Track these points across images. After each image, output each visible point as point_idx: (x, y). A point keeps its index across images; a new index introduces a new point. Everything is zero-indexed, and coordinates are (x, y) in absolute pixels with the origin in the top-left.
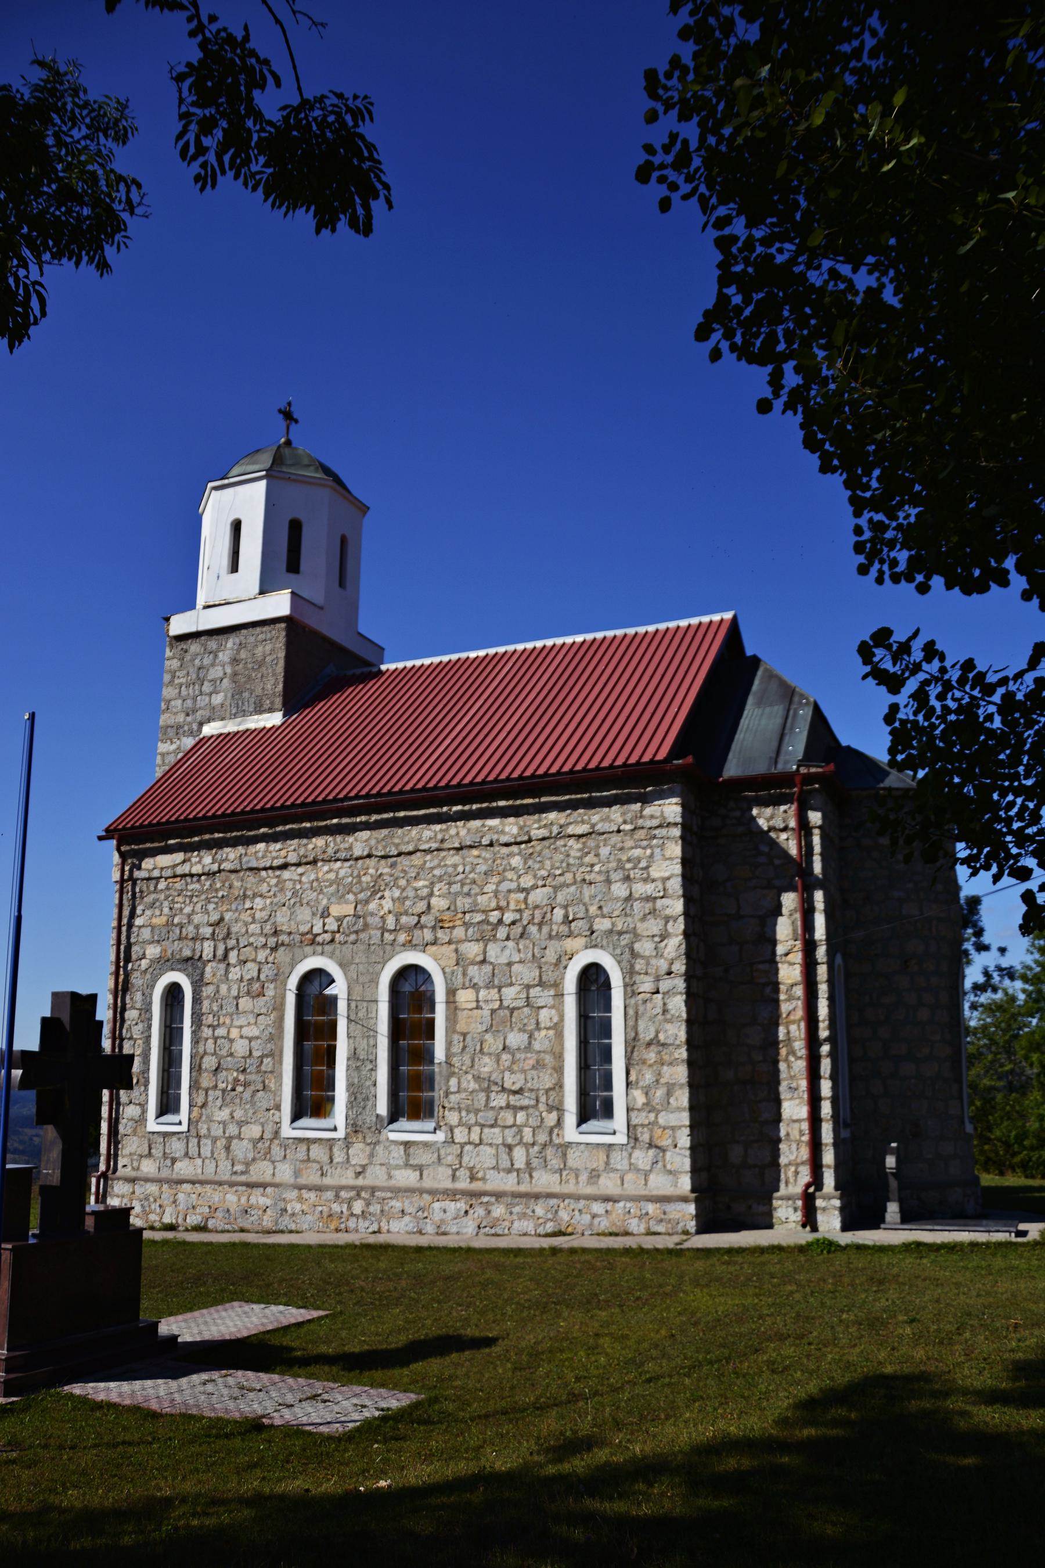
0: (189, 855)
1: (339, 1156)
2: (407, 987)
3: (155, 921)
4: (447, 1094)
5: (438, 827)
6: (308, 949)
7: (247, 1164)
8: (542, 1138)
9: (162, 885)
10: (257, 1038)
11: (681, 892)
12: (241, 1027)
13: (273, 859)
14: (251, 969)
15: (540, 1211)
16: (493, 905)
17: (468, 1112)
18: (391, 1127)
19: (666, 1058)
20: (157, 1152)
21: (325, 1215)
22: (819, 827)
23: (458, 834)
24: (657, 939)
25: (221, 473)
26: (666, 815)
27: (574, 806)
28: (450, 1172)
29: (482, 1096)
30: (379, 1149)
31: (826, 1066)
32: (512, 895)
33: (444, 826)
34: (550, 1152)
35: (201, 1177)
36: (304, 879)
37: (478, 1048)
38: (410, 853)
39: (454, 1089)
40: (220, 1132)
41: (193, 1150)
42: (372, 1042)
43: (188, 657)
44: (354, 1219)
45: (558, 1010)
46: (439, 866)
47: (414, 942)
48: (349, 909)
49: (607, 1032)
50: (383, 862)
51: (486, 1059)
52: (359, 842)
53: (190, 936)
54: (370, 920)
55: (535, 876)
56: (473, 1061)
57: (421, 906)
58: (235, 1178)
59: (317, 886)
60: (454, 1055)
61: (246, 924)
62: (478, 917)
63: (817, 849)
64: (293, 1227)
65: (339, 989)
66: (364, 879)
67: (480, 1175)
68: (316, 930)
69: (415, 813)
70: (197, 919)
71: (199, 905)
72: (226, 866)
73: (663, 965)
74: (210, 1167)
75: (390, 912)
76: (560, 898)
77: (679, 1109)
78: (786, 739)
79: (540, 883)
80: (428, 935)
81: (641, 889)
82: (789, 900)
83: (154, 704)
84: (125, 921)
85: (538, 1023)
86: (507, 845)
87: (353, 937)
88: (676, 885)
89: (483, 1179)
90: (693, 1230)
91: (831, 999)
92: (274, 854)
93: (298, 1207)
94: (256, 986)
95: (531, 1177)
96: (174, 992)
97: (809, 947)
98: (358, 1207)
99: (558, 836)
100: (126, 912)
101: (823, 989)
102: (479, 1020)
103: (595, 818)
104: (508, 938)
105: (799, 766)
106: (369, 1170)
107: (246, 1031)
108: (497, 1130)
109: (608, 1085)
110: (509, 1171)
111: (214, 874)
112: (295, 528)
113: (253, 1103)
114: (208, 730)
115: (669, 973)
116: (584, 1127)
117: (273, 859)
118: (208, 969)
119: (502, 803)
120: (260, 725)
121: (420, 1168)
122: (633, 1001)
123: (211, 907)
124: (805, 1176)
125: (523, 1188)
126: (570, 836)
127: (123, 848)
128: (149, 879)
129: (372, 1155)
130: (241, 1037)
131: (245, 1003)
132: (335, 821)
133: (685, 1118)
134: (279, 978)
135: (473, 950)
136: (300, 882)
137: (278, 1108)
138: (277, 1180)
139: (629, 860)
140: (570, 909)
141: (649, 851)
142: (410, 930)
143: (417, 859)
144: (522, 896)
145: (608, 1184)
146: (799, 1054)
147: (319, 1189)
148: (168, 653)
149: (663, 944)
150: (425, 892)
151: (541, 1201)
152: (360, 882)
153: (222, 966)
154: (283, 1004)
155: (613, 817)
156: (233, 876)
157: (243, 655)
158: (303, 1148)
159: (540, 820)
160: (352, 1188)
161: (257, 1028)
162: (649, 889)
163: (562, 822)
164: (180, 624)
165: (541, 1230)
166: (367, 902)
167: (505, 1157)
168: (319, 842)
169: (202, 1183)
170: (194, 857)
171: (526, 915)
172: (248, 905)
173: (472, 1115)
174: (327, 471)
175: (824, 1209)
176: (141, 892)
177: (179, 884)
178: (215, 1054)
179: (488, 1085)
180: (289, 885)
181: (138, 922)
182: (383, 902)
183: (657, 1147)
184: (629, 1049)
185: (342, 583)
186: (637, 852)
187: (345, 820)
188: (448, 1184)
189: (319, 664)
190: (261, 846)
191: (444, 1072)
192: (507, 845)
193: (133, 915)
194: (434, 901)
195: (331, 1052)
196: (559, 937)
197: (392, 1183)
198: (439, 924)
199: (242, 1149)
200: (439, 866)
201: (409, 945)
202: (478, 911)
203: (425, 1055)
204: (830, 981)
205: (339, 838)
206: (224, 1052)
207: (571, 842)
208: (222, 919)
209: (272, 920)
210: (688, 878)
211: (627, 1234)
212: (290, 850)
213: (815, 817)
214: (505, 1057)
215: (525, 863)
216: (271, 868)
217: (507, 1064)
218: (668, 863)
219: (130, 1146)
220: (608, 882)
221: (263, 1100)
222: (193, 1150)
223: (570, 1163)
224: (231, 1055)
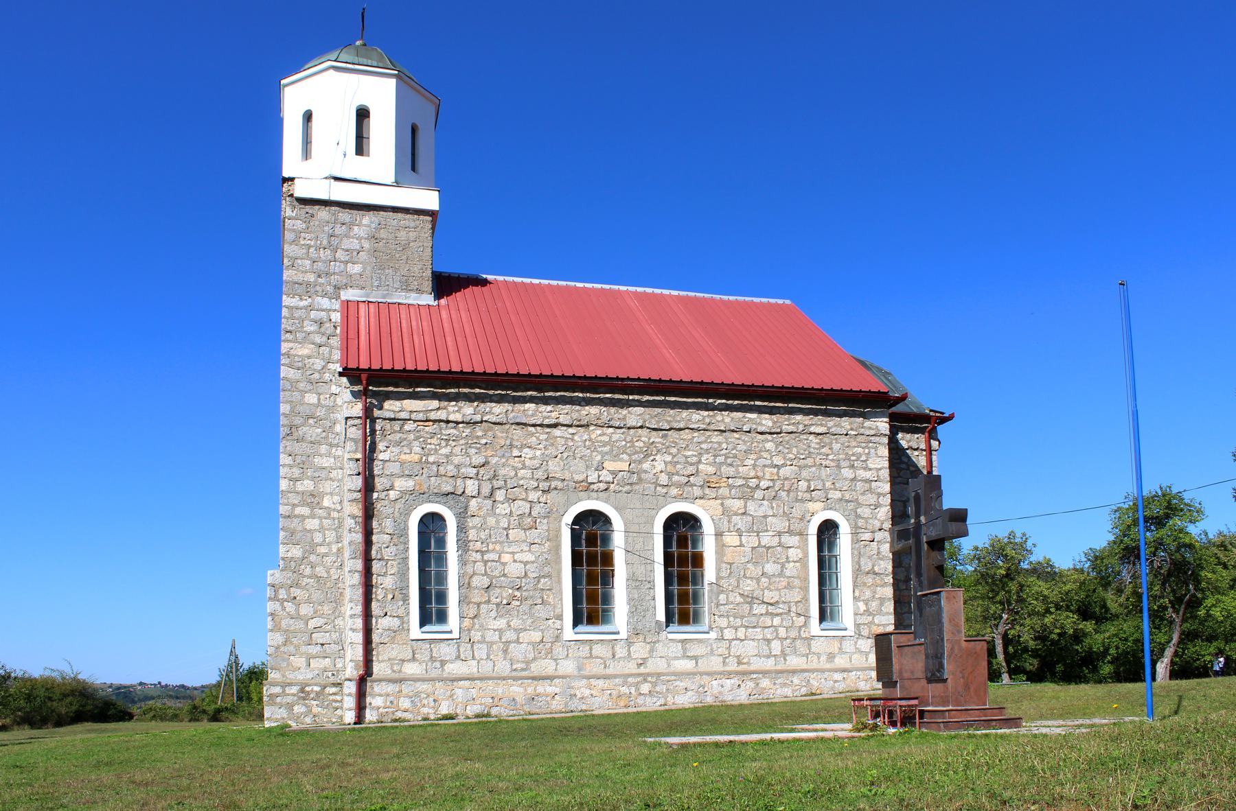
16: (752, 474)
17: (735, 617)
33: (711, 413)
51: (749, 581)
57: (691, 470)
62: (740, 482)
76: (805, 474)
80: (697, 492)
86: (761, 433)
103: (830, 424)
125: (779, 667)
135: (737, 504)
142: (679, 485)
143: (686, 435)
150: (695, 459)
171: (778, 483)
179: (751, 599)
192: (761, 433)
194: (701, 467)
196: (802, 501)
198: (707, 484)
200: (705, 442)
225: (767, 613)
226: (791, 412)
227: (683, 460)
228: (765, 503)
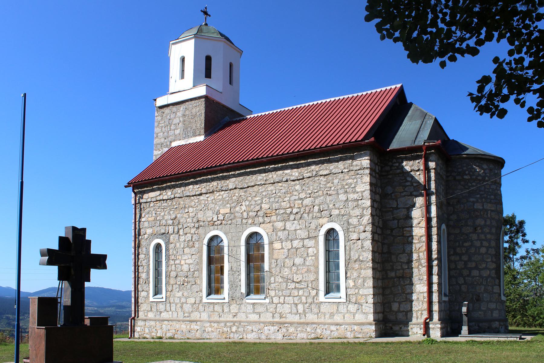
0: (162, 192)
1: (226, 310)
2: (253, 241)
3: (149, 219)
4: (270, 284)
5: (264, 175)
6: (212, 228)
7: (190, 313)
8: (310, 300)
9: (152, 204)
10: (192, 264)
11: (369, 197)
12: (185, 260)
13: (196, 191)
14: (189, 236)
15: (309, 330)
16: (288, 206)
17: (279, 291)
18: (247, 298)
19: (363, 266)
20: (154, 309)
21: (221, 332)
22: (434, 169)
23: (272, 177)
24: (359, 217)
25: (176, 37)
26: (363, 164)
27: (322, 162)
28: (272, 315)
29: (285, 284)
30: (242, 306)
31: (435, 270)
32: (296, 202)
33: (267, 174)
34: (313, 306)
35: (171, 319)
36: (209, 199)
37: (283, 265)
38: (253, 186)
39: (272, 281)
40: (178, 301)
41: (168, 309)
42: (238, 264)
43: (164, 115)
44: (233, 334)
45: (316, 248)
46: (265, 191)
47: (255, 223)
48: (228, 211)
49: (337, 256)
50: (241, 190)
51: (286, 269)
52: (231, 183)
53: (164, 224)
54: (236, 214)
55: (306, 193)
56: (280, 270)
57: (258, 208)
58: (184, 319)
59: (215, 202)
60: (273, 268)
61: (186, 219)
62: (282, 211)
63: (433, 178)
64: (208, 337)
65: (225, 243)
66: (233, 198)
67: (284, 316)
68: (214, 220)
69: (254, 169)
70: (166, 217)
71: (167, 212)
72: (177, 195)
73: (362, 228)
74: (175, 315)
75: (245, 211)
77: (369, 287)
78: (420, 132)
79: (308, 196)
80: (261, 220)
81: (351, 196)
82: (420, 201)
83: (151, 134)
84: (137, 220)
85: (308, 254)
86: (293, 181)
87: (230, 222)
88: (367, 194)
89: (285, 317)
90: (374, 336)
91: (439, 242)
92: (196, 189)
93: (210, 329)
94: (191, 243)
95: (305, 316)
96: (158, 246)
97: (429, 220)
98: (234, 329)
99: (316, 176)
100: (138, 216)
101: (435, 238)
102: (283, 253)
103: (332, 168)
104: (295, 220)
105: (425, 142)
106: (239, 315)
107: (187, 261)
108: (291, 298)
109: (338, 279)
110: (296, 314)
111: (172, 199)
112: (208, 59)
113: (191, 289)
114: (174, 144)
115: (365, 232)
116: (328, 296)
117: (196, 191)
118: (171, 237)
119: (291, 163)
120: (195, 141)
121: (259, 314)
122: (348, 243)
123: (172, 212)
124: (425, 315)
125: (302, 321)
126: (321, 176)
127: (135, 191)
128: (146, 202)
129: (239, 309)
130: (186, 264)
131: (187, 250)
132: (221, 175)
133: (371, 291)
134: (200, 240)
135: (279, 225)
136: (207, 200)
137: (201, 291)
138: (202, 319)
139: (346, 185)
140: (321, 206)
141: (355, 180)
142: (253, 218)
144: (300, 202)
145: (338, 318)
146: (424, 265)
147: (218, 322)
148: (156, 114)
149: (362, 219)
151: (309, 326)
152: (232, 199)
153: (177, 236)
154: (202, 250)
155: (339, 166)
156: (180, 199)
157: (187, 113)
158: (212, 306)
159: (308, 170)
160: (232, 322)
161: (192, 260)
162: (355, 196)
163: (317, 170)
164: (161, 101)
165: (309, 337)
166: (235, 207)
167: (295, 308)
168: (215, 183)
169: (171, 321)
170: (164, 192)
172: (186, 211)
173: (280, 292)
174: (221, 35)
175: (433, 328)
176: (144, 208)
177: (159, 204)
178: (175, 271)
179: (287, 280)
180: (203, 202)
181: (143, 220)
182: (242, 207)
183: (359, 304)
184: (347, 263)
185: (230, 84)
186: (350, 181)
187: (225, 174)
188: (271, 320)
189: (219, 116)
190: (191, 186)
191: (269, 275)
192: (293, 181)
193: (140, 217)
194: (263, 205)
195: (222, 268)
196: (317, 218)
197: (248, 319)
198: (266, 215)
199: (187, 307)
200: (265, 191)
201: (253, 224)
202: (282, 209)
203: (260, 269)
204: (438, 235)
205: (223, 182)
206: (179, 270)
207: (322, 178)
208: (176, 217)
209: (196, 216)
210: (373, 192)
211: (346, 338)
212: (203, 187)
213: (432, 165)
214: (294, 268)
215: (302, 188)
216: (195, 195)
217: (295, 271)
218: (363, 185)
219: (143, 307)
220: (338, 194)
221: (195, 288)
222: (168, 309)
223: (322, 310)
224: (182, 271)
225: (295, 288)
226: (309, 164)
227: (253, 203)
228: (296, 222)
